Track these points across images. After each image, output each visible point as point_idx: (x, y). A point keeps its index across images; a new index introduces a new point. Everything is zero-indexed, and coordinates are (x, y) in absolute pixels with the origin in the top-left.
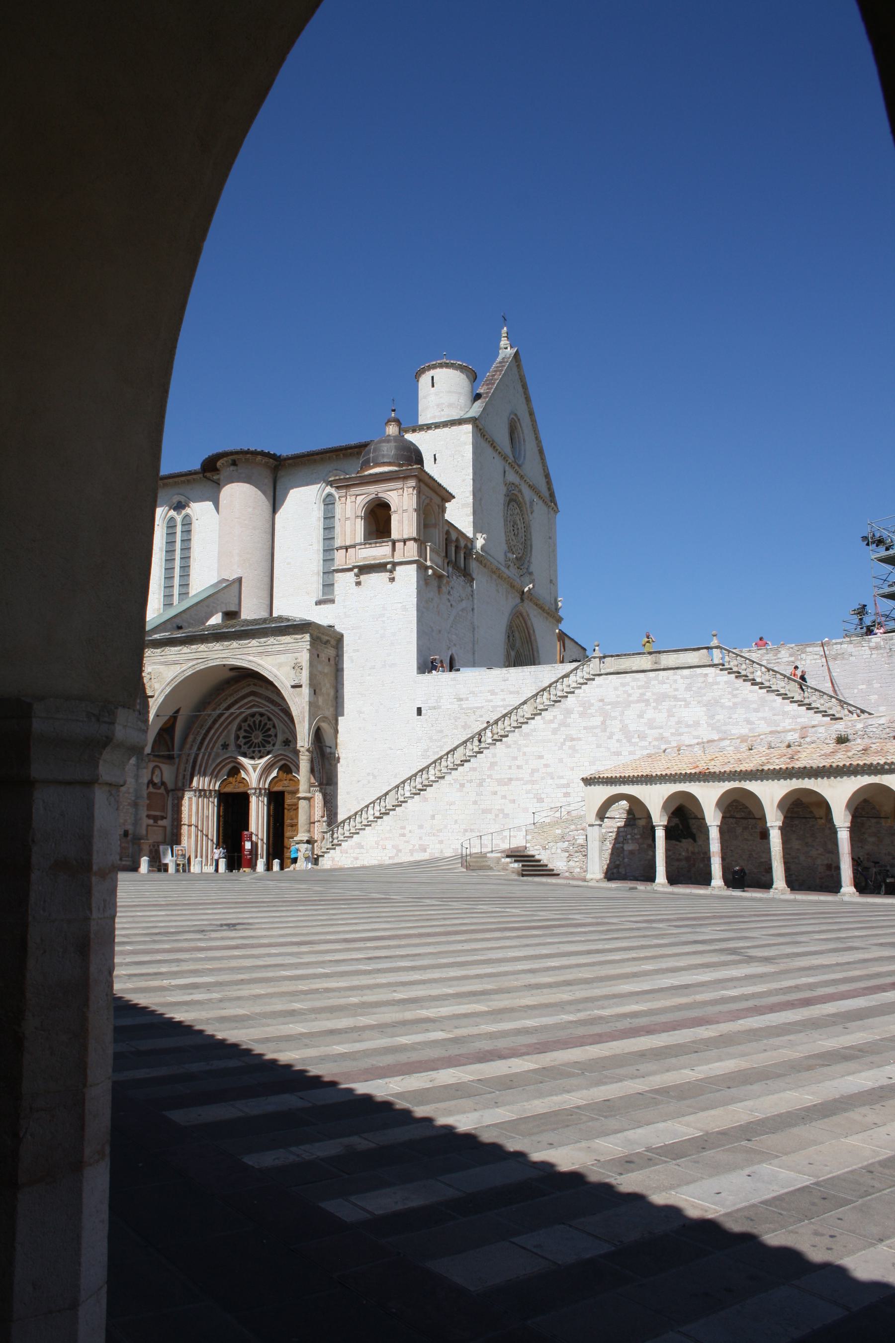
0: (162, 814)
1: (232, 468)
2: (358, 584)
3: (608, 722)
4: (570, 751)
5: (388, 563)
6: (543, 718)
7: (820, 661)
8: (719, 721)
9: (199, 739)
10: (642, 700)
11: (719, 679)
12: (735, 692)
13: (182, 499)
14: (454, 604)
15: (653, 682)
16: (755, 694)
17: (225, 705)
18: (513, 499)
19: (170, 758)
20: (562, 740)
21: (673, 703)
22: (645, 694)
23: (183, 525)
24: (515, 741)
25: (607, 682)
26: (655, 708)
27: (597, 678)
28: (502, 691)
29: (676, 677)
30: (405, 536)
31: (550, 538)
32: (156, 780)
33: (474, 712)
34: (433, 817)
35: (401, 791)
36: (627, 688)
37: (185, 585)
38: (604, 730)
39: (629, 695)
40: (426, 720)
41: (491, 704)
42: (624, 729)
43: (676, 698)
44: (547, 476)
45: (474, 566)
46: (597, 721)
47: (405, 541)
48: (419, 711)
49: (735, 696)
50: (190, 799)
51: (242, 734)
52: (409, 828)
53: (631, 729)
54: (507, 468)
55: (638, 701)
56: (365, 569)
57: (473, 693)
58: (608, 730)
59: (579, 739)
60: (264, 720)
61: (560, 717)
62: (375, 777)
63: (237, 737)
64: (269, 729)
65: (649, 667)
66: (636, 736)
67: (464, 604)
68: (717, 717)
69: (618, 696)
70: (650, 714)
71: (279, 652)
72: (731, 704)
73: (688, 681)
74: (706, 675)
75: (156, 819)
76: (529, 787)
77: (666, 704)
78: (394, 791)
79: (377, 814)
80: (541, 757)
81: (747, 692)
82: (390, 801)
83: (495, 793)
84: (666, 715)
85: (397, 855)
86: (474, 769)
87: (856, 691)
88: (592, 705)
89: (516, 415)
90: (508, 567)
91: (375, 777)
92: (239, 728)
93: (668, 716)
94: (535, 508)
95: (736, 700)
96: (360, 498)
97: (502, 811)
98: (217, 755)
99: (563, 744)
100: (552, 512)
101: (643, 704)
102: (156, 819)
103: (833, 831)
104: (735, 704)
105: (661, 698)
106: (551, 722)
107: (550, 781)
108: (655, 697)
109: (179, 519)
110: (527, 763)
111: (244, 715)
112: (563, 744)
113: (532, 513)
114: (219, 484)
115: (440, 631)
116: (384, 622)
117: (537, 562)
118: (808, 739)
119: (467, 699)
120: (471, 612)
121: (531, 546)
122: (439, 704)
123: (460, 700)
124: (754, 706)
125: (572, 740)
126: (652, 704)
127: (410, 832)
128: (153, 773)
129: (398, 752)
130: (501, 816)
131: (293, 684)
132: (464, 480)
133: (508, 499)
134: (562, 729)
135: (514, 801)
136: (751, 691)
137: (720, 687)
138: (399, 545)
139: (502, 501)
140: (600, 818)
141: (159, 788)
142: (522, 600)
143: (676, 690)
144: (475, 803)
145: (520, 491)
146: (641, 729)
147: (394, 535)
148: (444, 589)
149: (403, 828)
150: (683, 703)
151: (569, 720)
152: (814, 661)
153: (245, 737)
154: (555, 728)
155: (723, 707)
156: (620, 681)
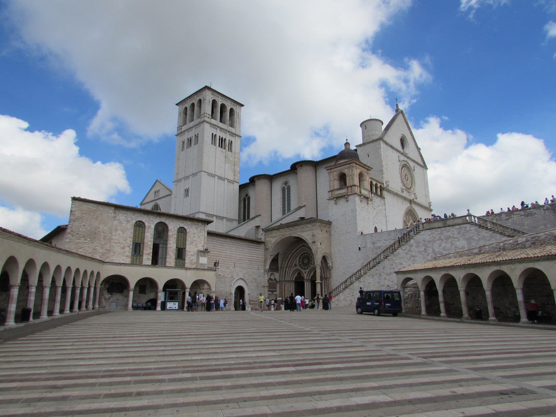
0: (275, 290)
1: (300, 167)
2: (336, 204)
3: (427, 249)
4: (413, 261)
5: (346, 195)
6: (402, 249)
7: (520, 217)
8: (473, 246)
9: (287, 263)
10: (440, 239)
11: (472, 228)
12: (479, 233)
13: (287, 180)
14: (375, 208)
15: (444, 232)
16: (488, 234)
17: (294, 251)
18: (405, 166)
19: (277, 270)
20: (409, 257)
21: (453, 240)
22: (441, 237)
23: (287, 189)
25: (426, 233)
26: (446, 242)
27: (421, 232)
28: (389, 239)
29: (453, 229)
30: (351, 185)
31: (424, 179)
32: (272, 278)
33: (379, 248)
35: (352, 279)
36: (434, 235)
37: (289, 210)
38: (426, 252)
39: (435, 238)
41: (385, 244)
42: (434, 251)
43: (454, 238)
44: (421, 156)
45: (385, 193)
46: (423, 249)
47: (351, 187)
49: (479, 235)
50: (285, 284)
51: (301, 260)
52: (355, 293)
53: (436, 251)
54: (400, 155)
55: (438, 240)
56: (338, 198)
57: (378, 241)
58: (427, 252)
59: (416, 256)
60: (308, 255)
61: (408, 248)
62: (345, 274)
63: (299, 262)
64: (310, 258)
65: (442, 226)
66: (439, 254)
67: (380, 208)
68: (472, 244)
69: (430, 238)
70: (443, 245)
71: (308, 231)
72: (477, 238)
73: (458, 230)
74: (466, 227)
75: (272, 292)
77: (450, 240)
78: (349, 279)
79: (344, 288)
80: (402, 264)
81: (484, 233)
82: (348, 283)
83: (385, 279)
84: (450, 245)
85: (351, 303)
86: (377, 270)
87: (539, 229)
88: (420, 242)
89: (403, 135)
90: (403, 192)
91: (345, 274)
92: (300, 258)
93: (451, 245)
94: (416, 169)
95: (479, 237)
96: (335, 173)
98: (293, 268)
99: (410, 258)
100: (425, 170)
101: (441, 241)
102: (272, 292)
103: (514, 290)
104: (479, 238)
105: (448, 238)
106: (405, 250)
108: (445, 238)
109: (286, 187)
110: (397, 267)
111: (301, 254)
112: (410, 258)
113: (414, 170)
114: (297, 173)
115: (369, 219)
116: (345, 217)
117: (418, 189)
118: (482, 252)
119: (376, 243)
120: (384, 210)
121: (415, 183)
123: (374, 243)
124: (488, 239)
125: (413, 256)
126: (445, 241)
128: (271, 276)
129: (353, 264)
131: (312, 241)
132: (379, 162)
133: (401, 167)
134: (409, 252)
136: (486, 233)
137: (472, 232)
138: (350, 188)
139: (398, 168)
140: (403, 288)
141: (274, 281)
142: (411, 204)
143: (454, 234)
144: (378, 283)
145: (408, 163)
146: (441, 251)
147: (348, 185)
148: (370, 202)
149: (353, 293)
150: (457, 239)
151: (412, 249)
152: (518, 218)
153: (302, 262)
154: (406, 253)
155: (474, 240)
156: (431, 232)
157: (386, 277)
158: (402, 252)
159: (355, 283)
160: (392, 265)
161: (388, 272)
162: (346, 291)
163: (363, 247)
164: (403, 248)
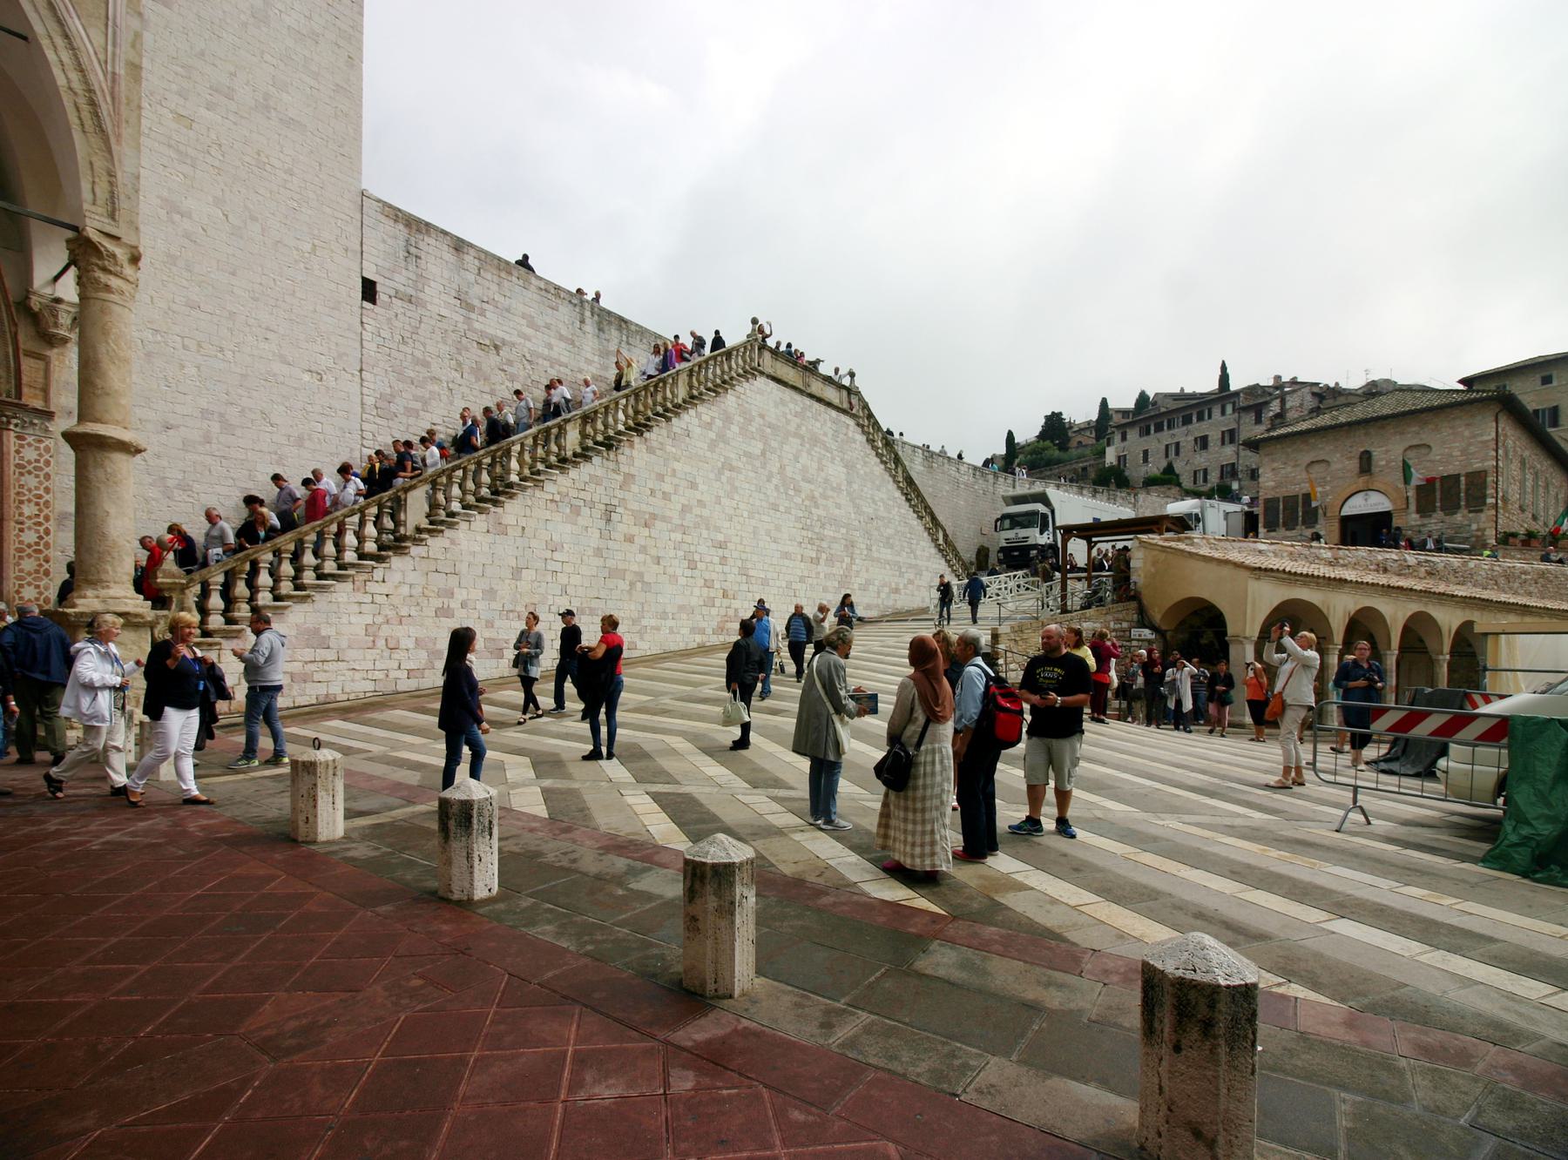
6: (699, 416)
24: (661, 443)
26: (809, 453)
33: (496, 347)
34: (517, 573)
38: (764, 466)
40: (389, 320)
48: (369, 291)
52: (461, 595)
76: (677, 536)
83: (630, 539)
91: (227, 427)
97: (640, 575)
107: (705, 533)
119: (482, 313)
122: (421, 295)
127: (464, 605)
129: (306, 377)
130: (639, 585)
135: (658, 561)
144: (598, 552)
156: (780, 394)
157: (635, 530)
158: (698, 430)
159: (463, 525)
160: (661, 477)
161: (644, 507)
162: (397, 577)
163: (398, 295)
164: (706, 418)
